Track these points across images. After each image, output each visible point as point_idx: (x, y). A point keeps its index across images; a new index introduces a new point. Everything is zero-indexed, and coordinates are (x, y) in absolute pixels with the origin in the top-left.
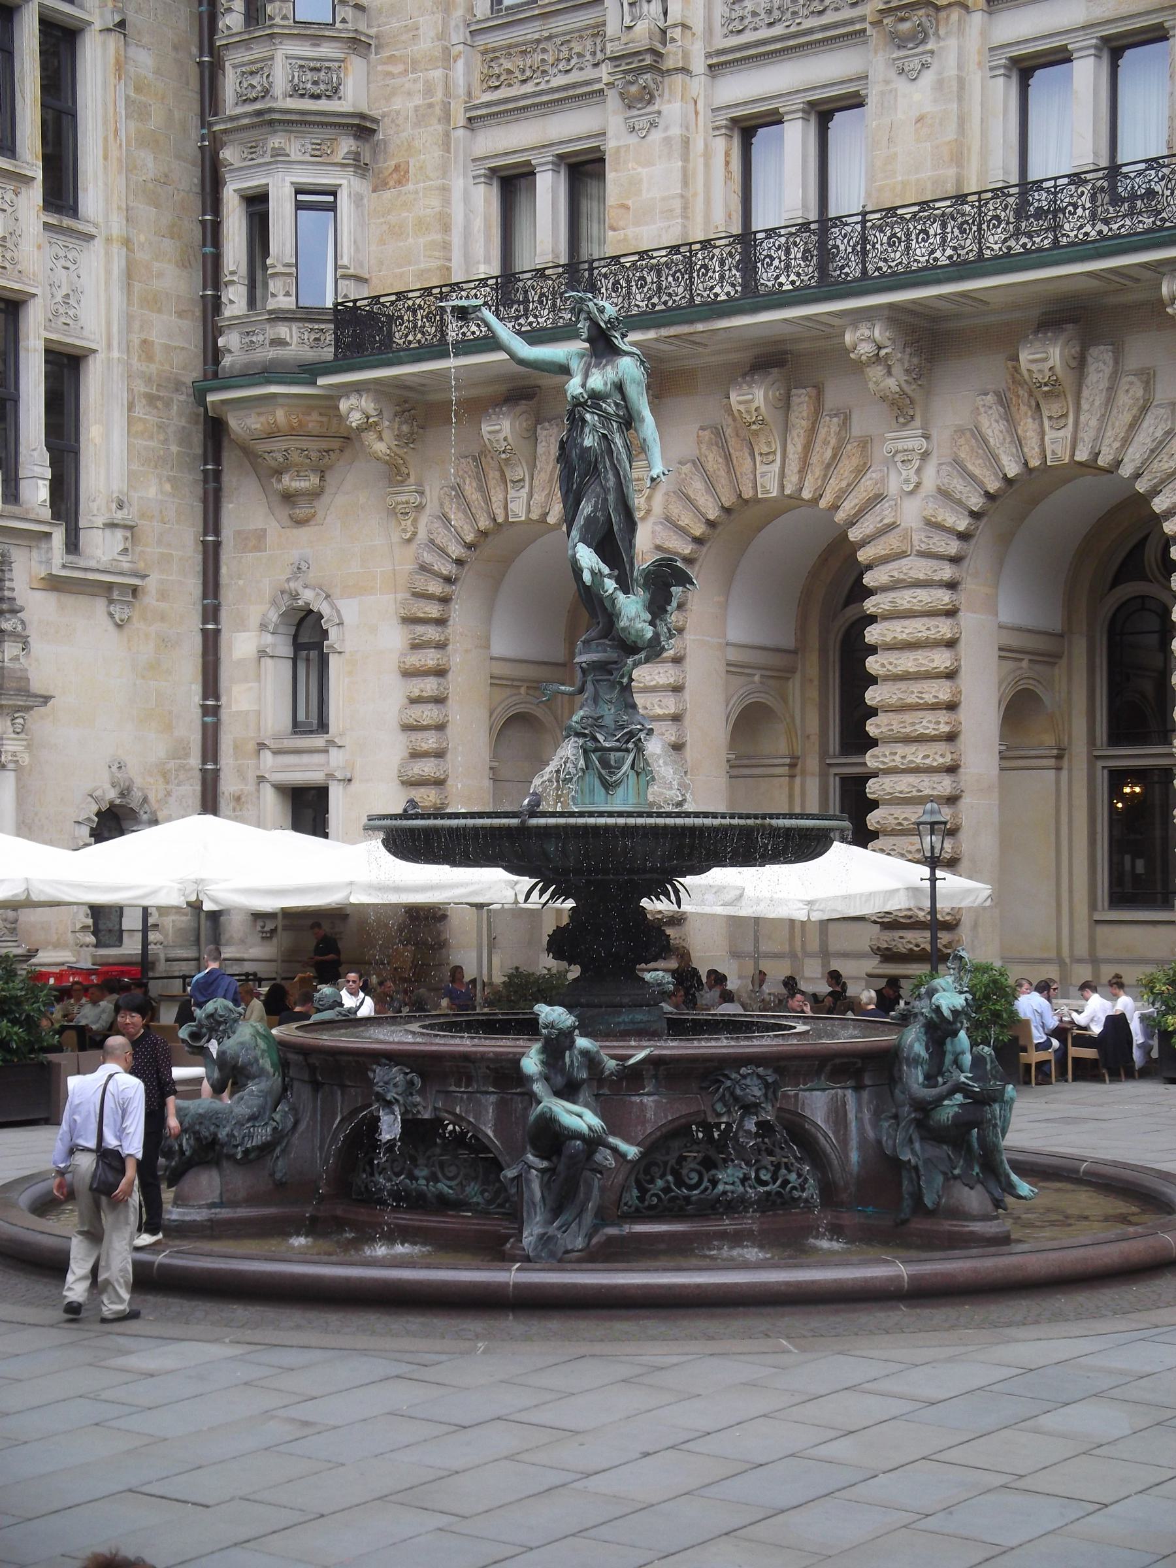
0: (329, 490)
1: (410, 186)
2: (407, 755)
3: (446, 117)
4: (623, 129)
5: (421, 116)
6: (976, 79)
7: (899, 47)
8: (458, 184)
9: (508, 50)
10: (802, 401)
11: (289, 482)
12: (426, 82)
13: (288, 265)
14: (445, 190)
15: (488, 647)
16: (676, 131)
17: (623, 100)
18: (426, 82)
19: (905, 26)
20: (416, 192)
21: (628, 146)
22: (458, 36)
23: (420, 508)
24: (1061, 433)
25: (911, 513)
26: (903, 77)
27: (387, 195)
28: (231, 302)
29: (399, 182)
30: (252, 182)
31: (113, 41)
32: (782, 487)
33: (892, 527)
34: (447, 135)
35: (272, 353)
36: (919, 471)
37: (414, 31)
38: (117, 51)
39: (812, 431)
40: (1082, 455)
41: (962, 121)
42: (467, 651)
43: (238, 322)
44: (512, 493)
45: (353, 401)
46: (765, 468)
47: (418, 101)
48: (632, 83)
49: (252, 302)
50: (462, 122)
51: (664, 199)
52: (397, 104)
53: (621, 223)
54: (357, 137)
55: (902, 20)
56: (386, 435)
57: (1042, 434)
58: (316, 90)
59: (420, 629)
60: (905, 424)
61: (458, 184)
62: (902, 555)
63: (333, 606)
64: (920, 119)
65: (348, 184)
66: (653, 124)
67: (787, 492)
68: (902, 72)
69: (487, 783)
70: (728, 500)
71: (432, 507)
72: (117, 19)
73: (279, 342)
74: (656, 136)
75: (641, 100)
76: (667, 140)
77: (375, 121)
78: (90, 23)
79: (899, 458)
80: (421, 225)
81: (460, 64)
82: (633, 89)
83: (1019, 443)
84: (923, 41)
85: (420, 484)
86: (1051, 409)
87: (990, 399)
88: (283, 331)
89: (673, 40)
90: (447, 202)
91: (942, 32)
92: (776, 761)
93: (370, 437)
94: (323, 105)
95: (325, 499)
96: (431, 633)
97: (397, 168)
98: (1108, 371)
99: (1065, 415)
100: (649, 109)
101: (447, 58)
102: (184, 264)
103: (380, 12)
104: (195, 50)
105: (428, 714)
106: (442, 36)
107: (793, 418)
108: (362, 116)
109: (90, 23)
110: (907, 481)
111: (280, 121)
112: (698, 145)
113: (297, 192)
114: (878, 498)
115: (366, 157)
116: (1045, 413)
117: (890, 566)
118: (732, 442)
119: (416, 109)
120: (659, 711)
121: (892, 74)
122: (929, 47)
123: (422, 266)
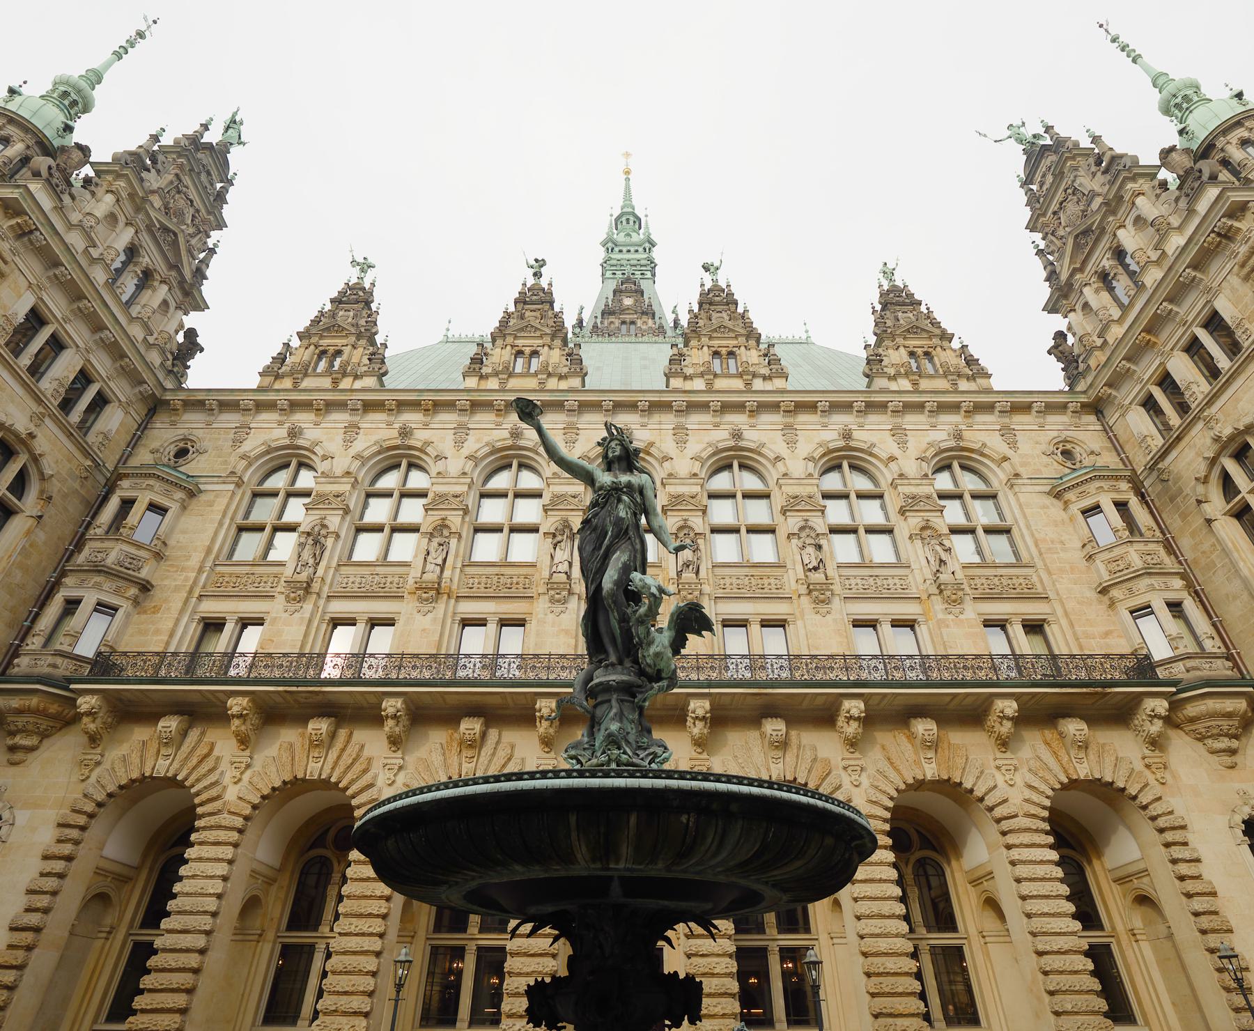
0: (42, 749)
2: (23, 910)
3: (191, 591)
8: (185, 619)
9: (231, 575)
10: (343, 733)
11: (20, 740)
13: (77, 632)
14: (178, 621)
15: (101, 849)
16: (307, 615)
22: (209, 564)
23: (98, 764)
27: (144, 617)
28: (33, 643)
29: (154, 613)
30: (74, 593)
31: (31, 522)
32: (320, 775)
35: (49, 670)
36: (395, 775)
37: (188, 558)
38: (31, 526)
42: (90, 849)
43: (31, 653)
44: (160, 761)
45: (88, 698)
49: (45, 645)
50: (196, 595)
52: (166, 582)
54: (140, 590)
56: (99, 721)
57: (460, 765)
58: (129, 566)
59: (67, 831)
61: (185, 619)
63: (12, 813)
64: (424, 630)
65: (125, 606)
67: (323, 777)
69: (66, 934)
71: (106, 765)
72: (39, 514)
73: (55, 666)
75: (294, 599)
76: (302, 618)
77: (152, 586)
78: (23, 511)
79: (388, 767)
81: (205, 574)
82: (292, 595)
85: (103, 750)
86: (467, 753)
87: (438, 746)
88: (59, 661)
92: (254, 932)
93: (85, 720)
94: (130, 572)
95: (36, 754)
96: (74, 833)
97: (154, 607)
101: (200, 570)
102: (10, 625)
103: (173, 548)
104: (67, 543)
105: (51, 883)
108: (148, 582)
109: (23, 511)
110: (389, 779)
111: (105, 572)
112: (315, 624)
113: (98, 604)
114: (371, 786)
115: (140, 600)
116: (464, 754)
120: (212, 892)
121: (415, 612)
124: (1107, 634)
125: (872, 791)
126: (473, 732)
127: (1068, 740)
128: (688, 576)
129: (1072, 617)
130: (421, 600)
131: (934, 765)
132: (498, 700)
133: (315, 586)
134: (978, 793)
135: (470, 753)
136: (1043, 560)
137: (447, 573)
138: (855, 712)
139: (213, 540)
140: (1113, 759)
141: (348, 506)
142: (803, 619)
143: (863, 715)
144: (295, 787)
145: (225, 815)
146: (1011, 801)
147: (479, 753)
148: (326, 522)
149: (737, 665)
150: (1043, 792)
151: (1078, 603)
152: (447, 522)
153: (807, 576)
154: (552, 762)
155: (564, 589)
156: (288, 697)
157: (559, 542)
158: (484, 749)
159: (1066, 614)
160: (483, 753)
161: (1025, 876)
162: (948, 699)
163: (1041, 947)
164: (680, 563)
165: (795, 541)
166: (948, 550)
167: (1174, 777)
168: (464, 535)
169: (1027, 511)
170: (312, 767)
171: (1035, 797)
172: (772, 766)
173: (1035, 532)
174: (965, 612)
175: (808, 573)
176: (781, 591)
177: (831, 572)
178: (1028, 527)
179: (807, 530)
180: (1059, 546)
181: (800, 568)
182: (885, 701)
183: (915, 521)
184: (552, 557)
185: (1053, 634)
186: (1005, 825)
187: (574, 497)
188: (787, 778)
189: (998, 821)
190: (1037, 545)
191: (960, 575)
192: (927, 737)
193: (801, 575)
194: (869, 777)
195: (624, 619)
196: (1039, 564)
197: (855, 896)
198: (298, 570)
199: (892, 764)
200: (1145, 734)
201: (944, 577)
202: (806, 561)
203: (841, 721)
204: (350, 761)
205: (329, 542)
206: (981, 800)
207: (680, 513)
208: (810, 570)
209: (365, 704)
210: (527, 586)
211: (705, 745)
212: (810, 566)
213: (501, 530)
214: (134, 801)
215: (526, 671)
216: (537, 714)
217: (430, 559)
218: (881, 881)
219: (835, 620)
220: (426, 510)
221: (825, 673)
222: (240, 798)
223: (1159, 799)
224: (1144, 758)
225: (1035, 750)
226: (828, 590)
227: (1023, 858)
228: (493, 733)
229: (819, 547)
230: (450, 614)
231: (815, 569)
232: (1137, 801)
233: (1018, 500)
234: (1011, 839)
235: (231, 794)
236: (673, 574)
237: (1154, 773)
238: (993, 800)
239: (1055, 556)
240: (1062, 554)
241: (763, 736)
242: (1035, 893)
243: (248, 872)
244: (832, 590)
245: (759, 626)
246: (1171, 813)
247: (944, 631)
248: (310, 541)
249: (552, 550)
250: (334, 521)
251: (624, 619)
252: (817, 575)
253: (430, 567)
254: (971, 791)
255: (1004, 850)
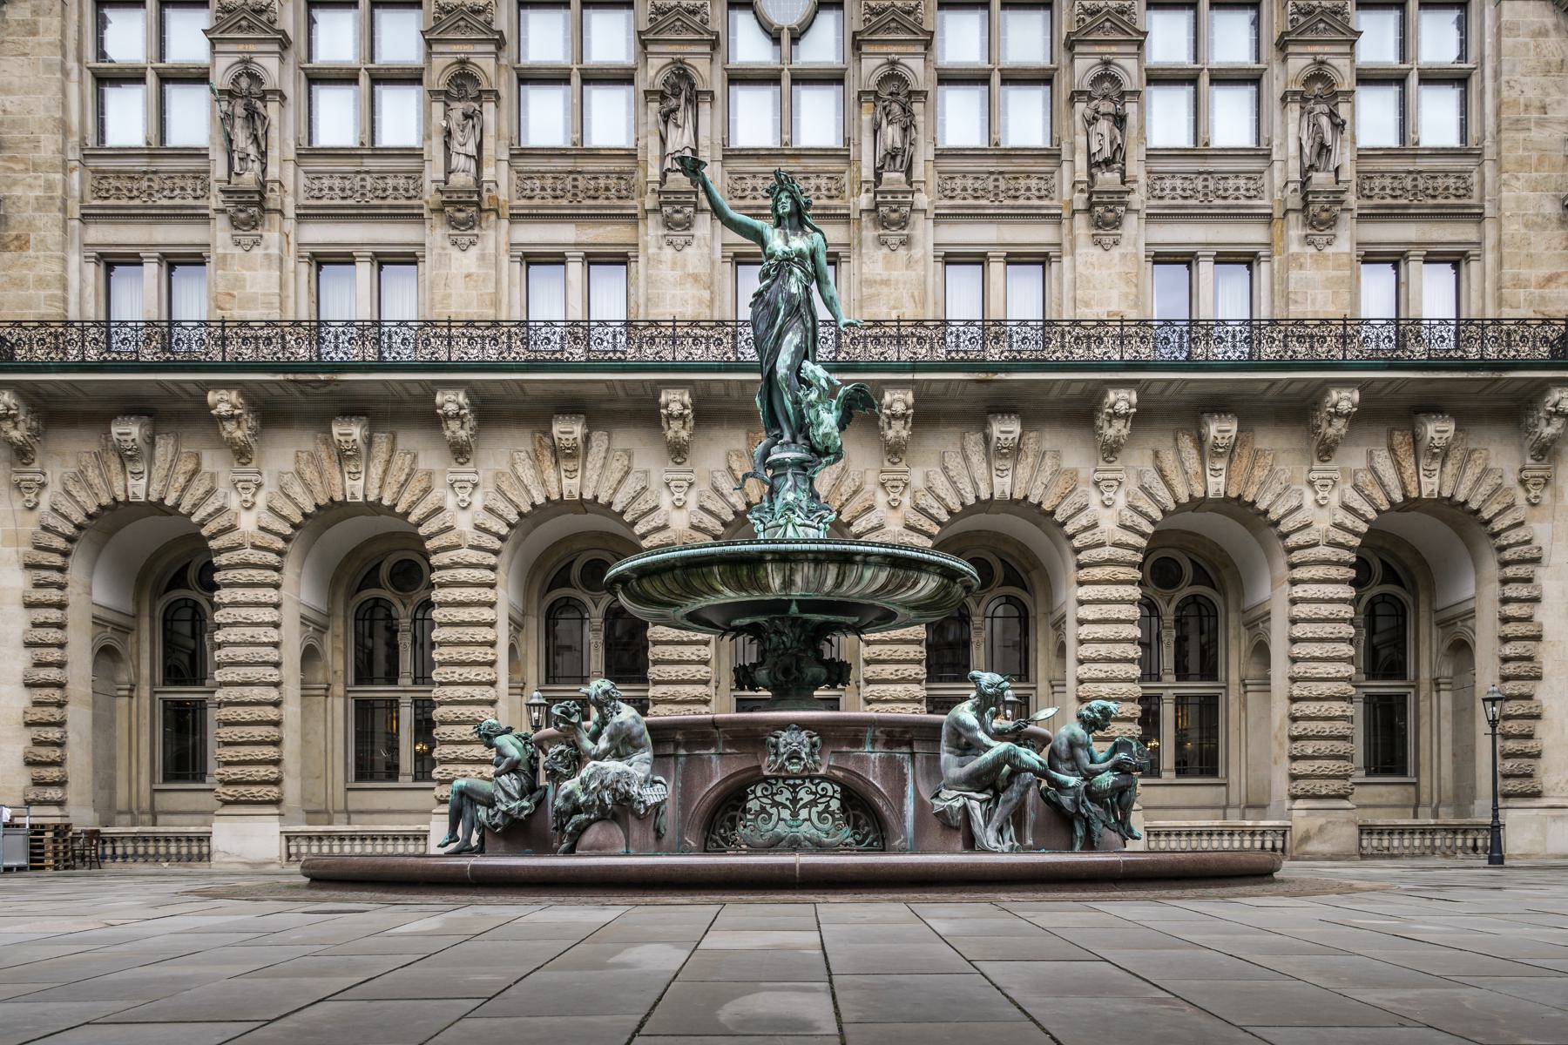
1: (31, 252)
3: (64, 209)
4: (229, 241)
5: (41, 205)
6: (505, 259)
7: (454, 228)
10: (382, 442)
12: (46, 180)
14: (64, 260)
16: (275, 251)
17: (232, 222)
18: (46, 180)
19: (461, 215)
20: (37, 258)
21: (233, 256)
24: (573, 481)
25: (464, 524)
26: (456, 247)
29: (20, 248)
32: (365, 496)
33: (450, 528)
34: (65, 222)
36: (470, 495)
39: (388, 462)
40: (588, 496)
41: (498, 282)
46: (352, 482)
47: (39, 192)
48: (241, 211)
51: (265, 295)
53: (228, 306)
55: (460, 210)
57: (560, 481)
60: (462, 464)
61: (74, 259)
62: (458, 547)
64: (468, 276)
66: (256, 243)
68: (455, 243)
70: (322, 500)
74: (257, 251)
75: (245, 224)
80: (41, 282)
82: (242, 216)
83: (544, 483)
84: (471, 228)
87: (523, 455)
89: (272, 190)
90: (65, 269)
91: (484, 225)
97: (18, 237)
98: (605, 447)
99: (576, 470)
100: (253, 232)
106: (63, 151)
107: (374, 451)
112: (290, 263)
114: (439, 510)
117: (450, 553)
118: (326, 464)
119: (37, 198)
121: (448, 244)
122: (476, 232)
123: (43, 311)
124: (1549, 280)
125: (1128, 513)
126: (571, 437)
127: (1422, 446)
128: (894, 178)
129: (1506, 250)
130: (453, 223)
131: (1222, 479)
132: (603, 390)
133: (273, 200)
134: (1273, 516)
135: (570, 465)
136: (1498, 142)
137: (488, 173)
138: (1122, 407)
139: (65, 107)
140: (1478, 470)
141: (283, 32)
142: (1073, 254)
143: (1134, 410)
144: (332, 512)
145: (249, 550)
146: (1316, 525)
147: (584, 467)
148: (254, 68)
149: (958, 336)
150: (1363, 515)
151: (1526, 225)
152: (470, 68)
153: (1091, 176)
154: (688, 477)
155: (687, 204)
156: (292, 389)
157: (674, 111)
158: (590, 459)
159: (1500, 244)
160: (589, 466)
161: (1303, 616)
162: (1264, 386)
163: (1296, 692)
164: (881, 153)
165: (1080, 107)
166: (1338, 126)
167: (1555, 496)
168: (503, 92)
169: (1507, 42)
170: (352, 486)
171: (1349, 520)
172: (996, 480)
173: (1504, 87)
174: (1336, 243)
175: (1094, 170)
176: (1045, 202)
177: (1136, 167)
178: (1497, 74)
179: (1106, 85)
180: (1534, 115)
181: (1081, 161)
182: (1172, 389)
183: (1299, 64)
184: (663, 141)
185: (1468, 278)
186: (1297, 556)
187: (690, 12)
188: (1015, 497)
189: (1290, 551)
190: (1498, 113)
191: (1348, 173)
192: (1218, 441)
193: (1082, 175)
194: (1128, 494)
195: (797, 402)
196: (1489, 153)
197: (1082, 637)
198: (237, 169)
199: (1163, 477)
200: (1535, 438)
201: (1320, 179)
202: (1095, 148)
203: (1102, 420)
204: (403, 478)
205: (272, 110)
206: (1277, 523)
207: (884, 49)
208: (1098, 165)
209: (405, 396)
210: (624, 193)
211: (903, 452)
212: (1099, 158)
213: (566, 81)
214: (110, 533)
215: (640, 347)
216: (664, 411)
217: (455, 146)
218: (1118, 621)
219: (1124, 256)
220: (429, 43)
221: (1089, 348)
222: (262, 529)
223: (1521, 524)
224: (1521, 471)
225: (1372, 459)
226: (1121, 204)
227: (1308, 595)
228: (599, 441)
229: (1120, 120)
230: (504, 247)
231: (1108, 163)
232: (1489, 528)
233: (1499, 16)
234: (1299, 573)
235: (248, 523)
236: (867, 173)
237: (1528, 491)
238: (1291, 524)
239: (1521, 136)
240: (1535, 134)
241: (987, 440)
242: (1310, 635)
243: (299, 619)
244: (1125, 204)
245: (1001, 265)
246: (1528, 542)
247: (1294, 274)
248: (240, 111)
249: (662, 128)
250: (270, 66)
251: (797, 402)
252: (1108, 175)
253: (459, 162)
254: (1266, 512)
255: (1287, 586)
